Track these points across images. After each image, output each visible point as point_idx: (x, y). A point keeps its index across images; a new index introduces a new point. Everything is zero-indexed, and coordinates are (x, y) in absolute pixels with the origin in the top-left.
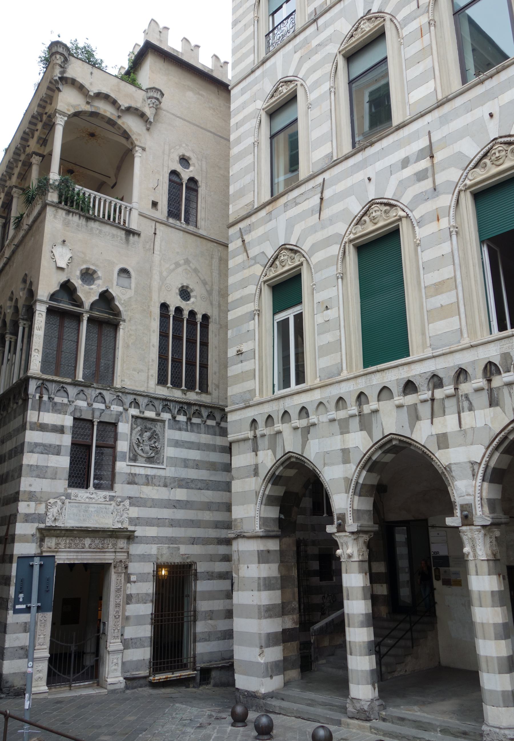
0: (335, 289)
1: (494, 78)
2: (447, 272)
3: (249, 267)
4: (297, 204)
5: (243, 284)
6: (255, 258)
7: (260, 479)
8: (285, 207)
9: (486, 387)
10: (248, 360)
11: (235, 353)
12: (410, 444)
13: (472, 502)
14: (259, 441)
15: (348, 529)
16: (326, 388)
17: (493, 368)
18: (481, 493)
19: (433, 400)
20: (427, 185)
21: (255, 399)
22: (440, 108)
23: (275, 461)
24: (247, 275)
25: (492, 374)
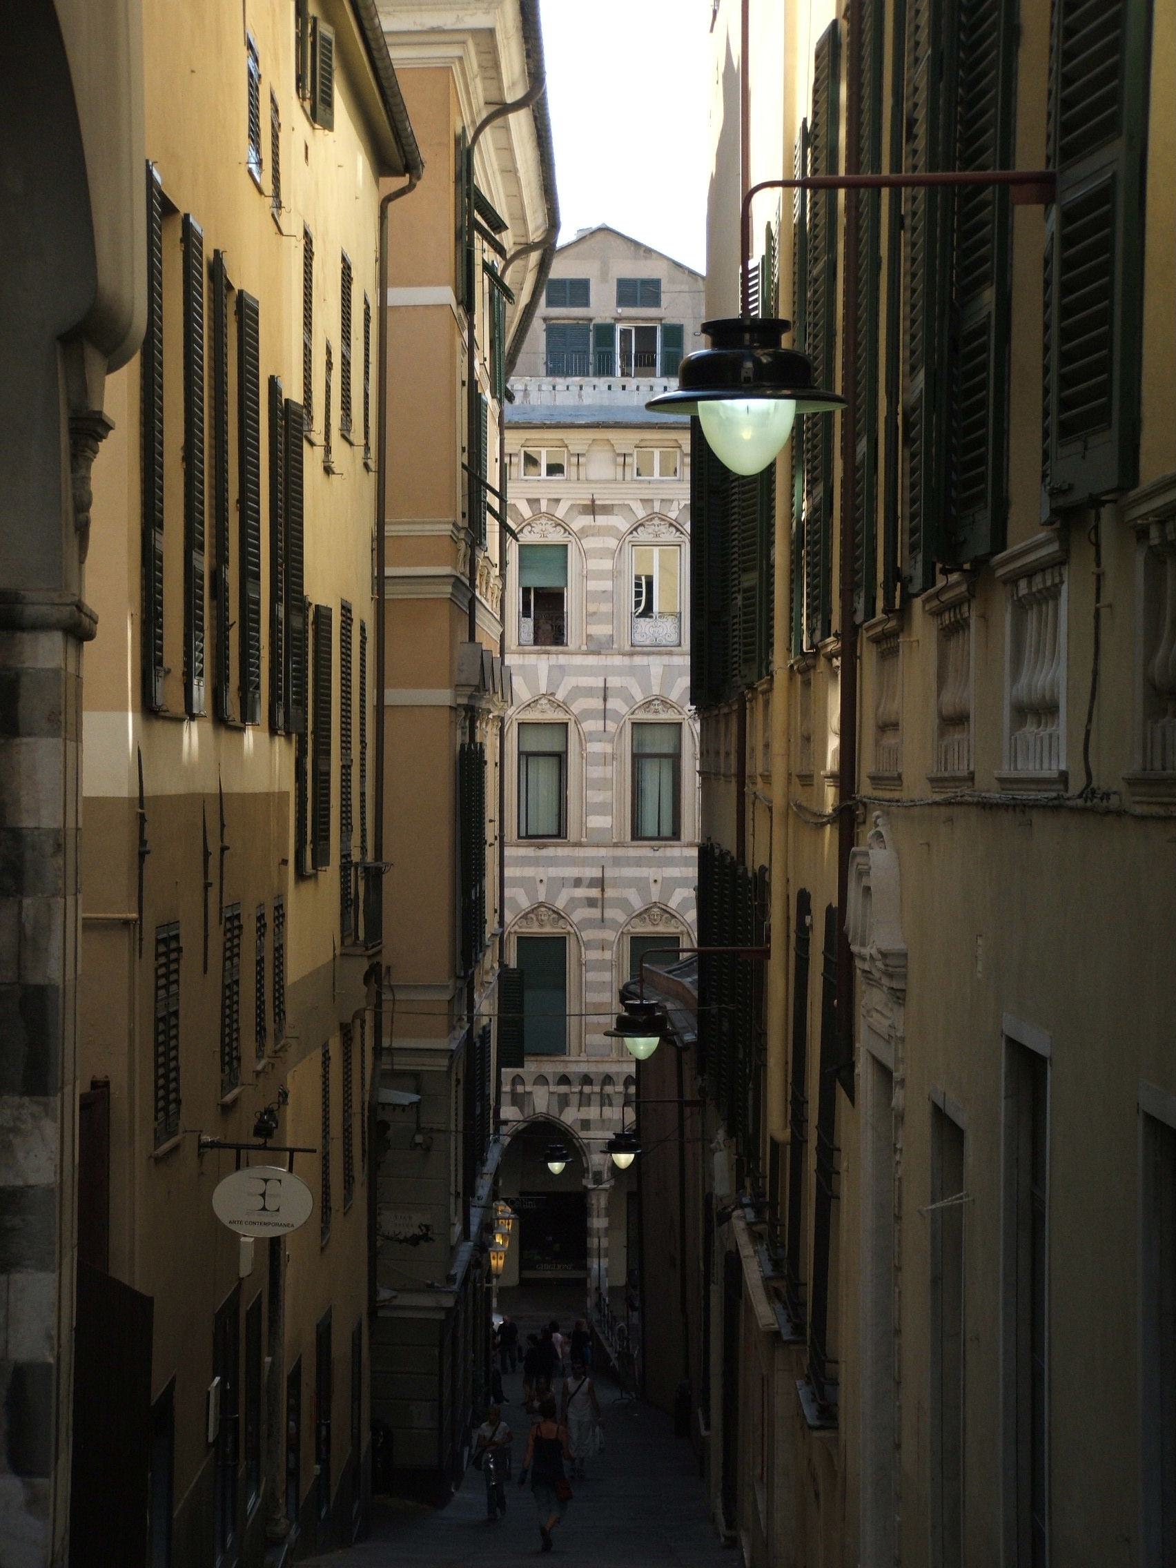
19: (581, 1093)
20: (595, 913)
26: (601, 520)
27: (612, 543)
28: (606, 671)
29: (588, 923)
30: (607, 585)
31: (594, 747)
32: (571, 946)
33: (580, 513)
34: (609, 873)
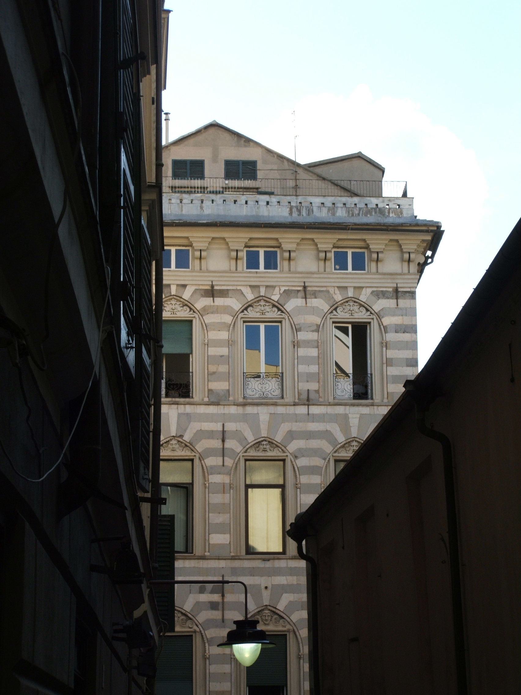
1: (271, 561)
20: (216, 615)
26: (219, 301)
27: (228, 319)
28: (225, 418)
30: (224, 351)
31: (215, 479)
32: (197, 642)
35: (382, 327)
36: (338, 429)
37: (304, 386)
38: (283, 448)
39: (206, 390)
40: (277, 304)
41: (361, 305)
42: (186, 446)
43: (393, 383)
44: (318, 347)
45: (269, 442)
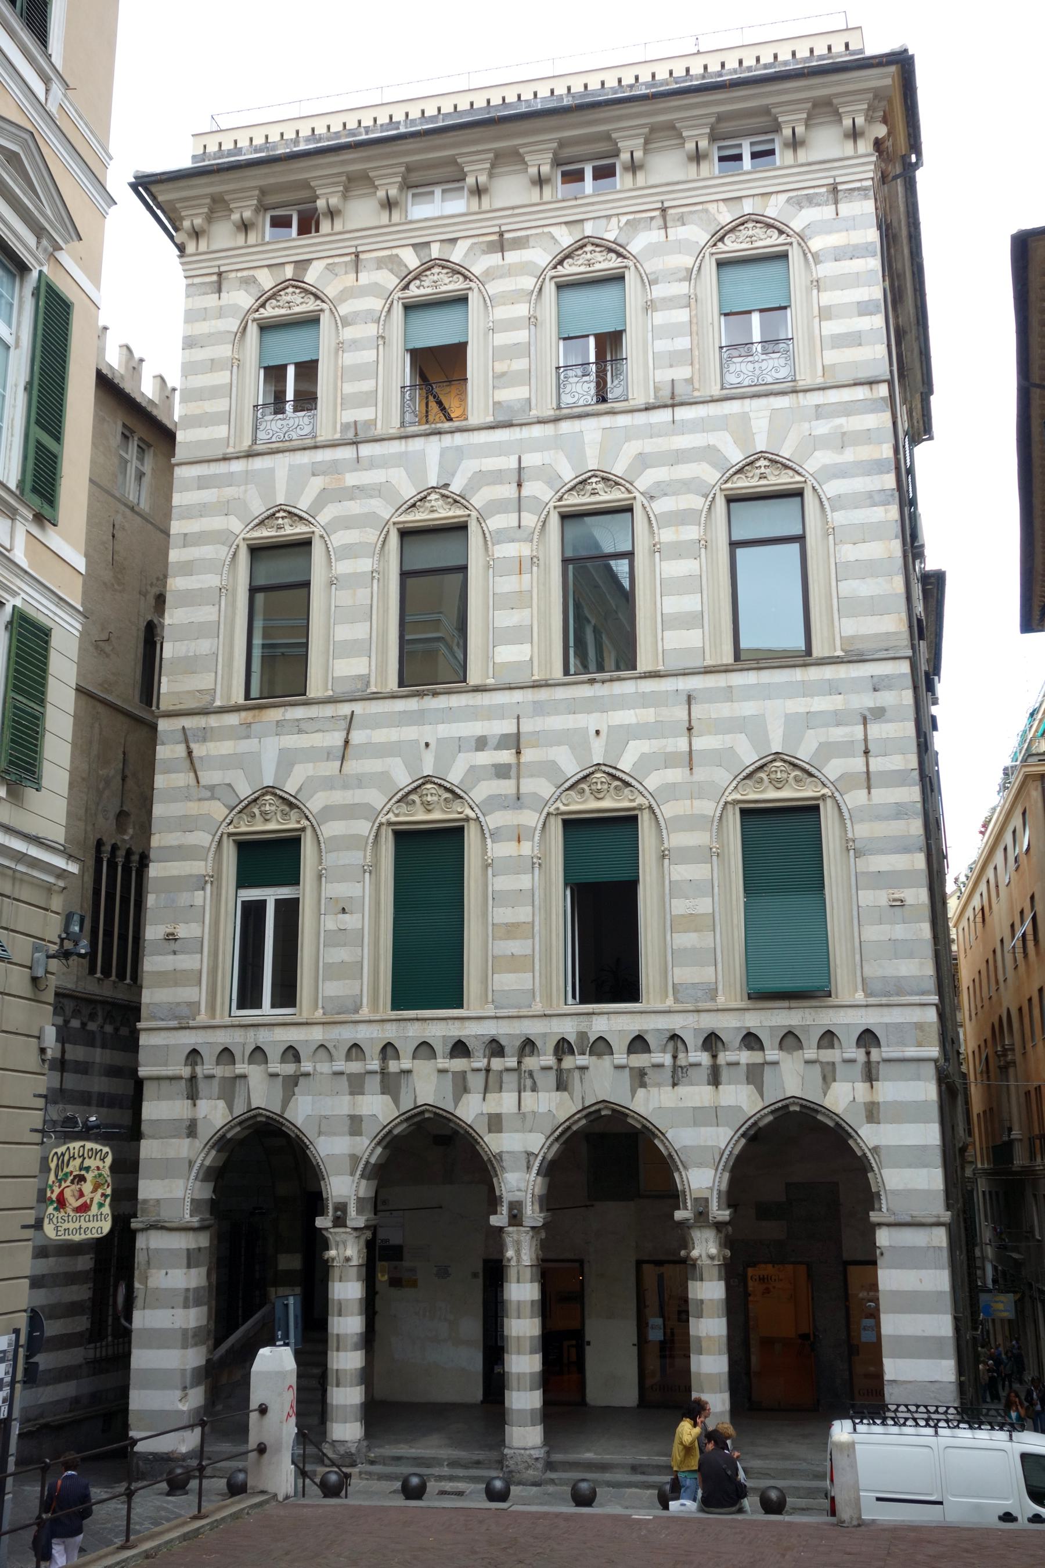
0: (359, 885)
1: (606, 685)
2: (523, 914)
3: (200, 800)
4: (300, 731)
5: (186, 824)
6: (212, 788)
7: (198, 1144)
8: (277, 726)
9: (555, 1067)
10: (188, 953)
11: (161, 935)
12: (450, 1120)
13: (523, 1199)
14: (202, 1085)
15: (349, 1223)
16: (333, 1026)
17: (566, 1045)
18: (533, 1189)
19: (488, 1070)
20: (506, 787)
21: (198, 1018)
22: (536, 689)
23: (230, 1118)
24: (194, 812)
25: (564, 1053)
26: (512, 257)
28: (520, 449)
29: (497, 802)
30: (522, 336)
32: (472, 837)
33: (484, 252)
34: (527, 727)
35: (809, 255)
36: (729, 439)
37: (664, 375)
38: (628, 485)
39: (491, 403)
40: (614, 246)
41: (769, 226)
42: (456, 501)
43: (833, 348)
44: (689, 306)
45: (603, 479)
